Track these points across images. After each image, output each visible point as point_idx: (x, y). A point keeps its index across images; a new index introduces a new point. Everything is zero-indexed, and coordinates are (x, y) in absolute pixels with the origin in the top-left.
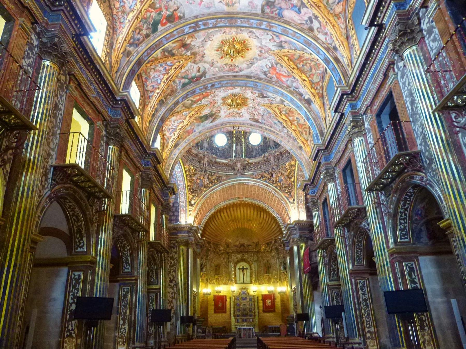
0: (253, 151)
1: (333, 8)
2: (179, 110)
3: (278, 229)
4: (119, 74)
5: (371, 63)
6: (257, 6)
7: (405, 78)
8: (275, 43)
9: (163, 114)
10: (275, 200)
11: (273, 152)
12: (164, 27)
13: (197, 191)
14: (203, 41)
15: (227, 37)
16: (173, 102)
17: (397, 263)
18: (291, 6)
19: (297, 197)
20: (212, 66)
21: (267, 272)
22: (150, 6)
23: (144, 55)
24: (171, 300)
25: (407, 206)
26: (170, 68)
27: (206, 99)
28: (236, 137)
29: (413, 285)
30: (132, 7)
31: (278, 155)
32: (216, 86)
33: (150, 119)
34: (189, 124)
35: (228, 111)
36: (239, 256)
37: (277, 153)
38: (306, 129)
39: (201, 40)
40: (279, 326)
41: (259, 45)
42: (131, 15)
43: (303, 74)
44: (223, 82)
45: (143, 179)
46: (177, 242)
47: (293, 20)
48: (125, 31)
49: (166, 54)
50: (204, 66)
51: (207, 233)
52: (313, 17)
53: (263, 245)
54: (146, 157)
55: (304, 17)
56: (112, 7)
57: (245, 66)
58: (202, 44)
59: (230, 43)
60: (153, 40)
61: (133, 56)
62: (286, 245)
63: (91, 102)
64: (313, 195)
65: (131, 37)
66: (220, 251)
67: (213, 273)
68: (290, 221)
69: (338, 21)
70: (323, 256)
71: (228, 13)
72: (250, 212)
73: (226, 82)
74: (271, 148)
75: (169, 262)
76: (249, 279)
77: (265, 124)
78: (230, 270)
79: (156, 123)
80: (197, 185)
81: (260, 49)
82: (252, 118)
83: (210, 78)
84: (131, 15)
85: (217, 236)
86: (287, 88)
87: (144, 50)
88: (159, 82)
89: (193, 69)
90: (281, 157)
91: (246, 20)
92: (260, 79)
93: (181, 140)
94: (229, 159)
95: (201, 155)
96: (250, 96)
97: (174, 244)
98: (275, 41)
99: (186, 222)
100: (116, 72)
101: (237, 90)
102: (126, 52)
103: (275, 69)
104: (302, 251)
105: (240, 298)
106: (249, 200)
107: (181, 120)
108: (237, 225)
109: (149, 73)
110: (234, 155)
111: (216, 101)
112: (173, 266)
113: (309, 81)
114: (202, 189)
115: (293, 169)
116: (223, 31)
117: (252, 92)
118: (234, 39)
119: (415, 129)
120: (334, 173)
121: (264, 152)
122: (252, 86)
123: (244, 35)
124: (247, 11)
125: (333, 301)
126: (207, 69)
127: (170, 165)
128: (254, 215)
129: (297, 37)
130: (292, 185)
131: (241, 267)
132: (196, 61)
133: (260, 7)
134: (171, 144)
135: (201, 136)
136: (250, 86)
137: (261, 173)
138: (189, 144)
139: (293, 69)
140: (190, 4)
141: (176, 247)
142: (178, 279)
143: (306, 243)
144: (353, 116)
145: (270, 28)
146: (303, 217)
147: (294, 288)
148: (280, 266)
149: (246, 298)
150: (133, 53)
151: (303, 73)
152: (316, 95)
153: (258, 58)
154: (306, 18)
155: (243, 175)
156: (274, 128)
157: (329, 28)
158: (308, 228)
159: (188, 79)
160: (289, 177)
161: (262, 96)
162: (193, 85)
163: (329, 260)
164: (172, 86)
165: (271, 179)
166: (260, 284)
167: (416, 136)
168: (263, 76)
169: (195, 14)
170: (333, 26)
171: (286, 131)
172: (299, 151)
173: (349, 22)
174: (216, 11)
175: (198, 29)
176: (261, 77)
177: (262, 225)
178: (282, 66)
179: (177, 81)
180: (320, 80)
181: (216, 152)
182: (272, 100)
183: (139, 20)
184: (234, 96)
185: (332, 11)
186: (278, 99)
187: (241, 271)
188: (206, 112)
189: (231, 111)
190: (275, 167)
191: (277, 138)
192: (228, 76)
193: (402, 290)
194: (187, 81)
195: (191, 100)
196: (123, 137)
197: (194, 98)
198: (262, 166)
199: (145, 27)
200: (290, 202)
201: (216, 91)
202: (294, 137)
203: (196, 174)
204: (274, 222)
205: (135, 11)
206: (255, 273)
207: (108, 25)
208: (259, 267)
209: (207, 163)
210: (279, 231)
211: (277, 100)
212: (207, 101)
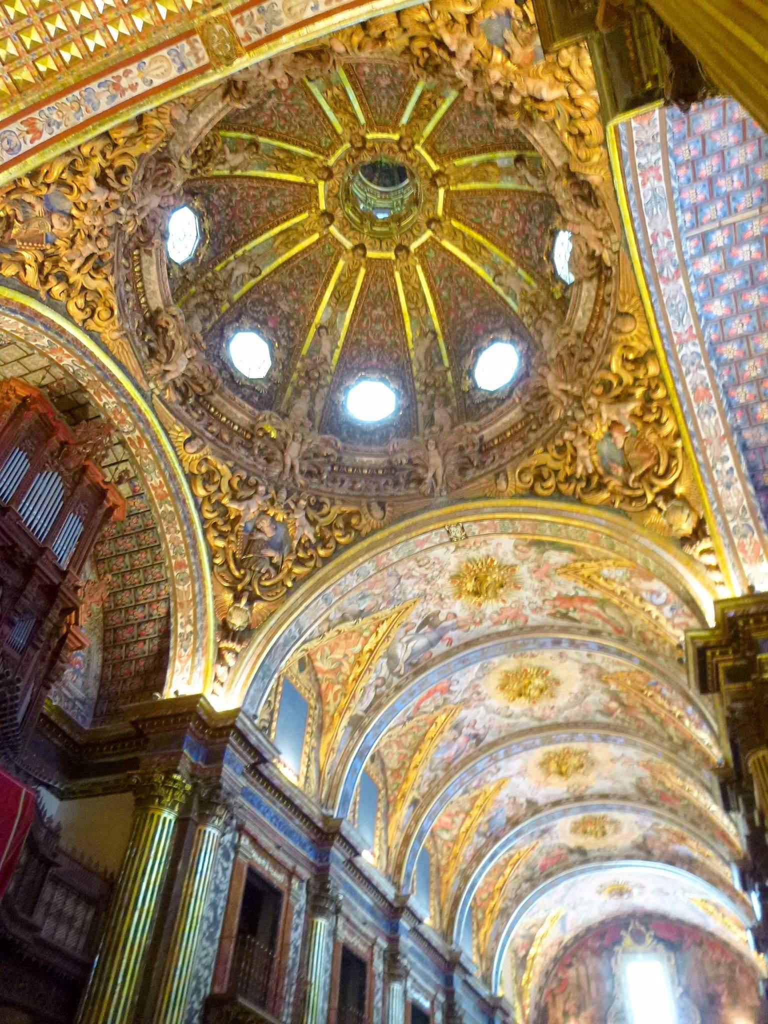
8: (466, 723)
41: (487, 702)
96: (453, 604)
103: (442, 693)
111: (534, 576)
117: (455, 616)
153: (477, 682)
161: (429, 621)
201: (540, 603)
212: (559, 584)
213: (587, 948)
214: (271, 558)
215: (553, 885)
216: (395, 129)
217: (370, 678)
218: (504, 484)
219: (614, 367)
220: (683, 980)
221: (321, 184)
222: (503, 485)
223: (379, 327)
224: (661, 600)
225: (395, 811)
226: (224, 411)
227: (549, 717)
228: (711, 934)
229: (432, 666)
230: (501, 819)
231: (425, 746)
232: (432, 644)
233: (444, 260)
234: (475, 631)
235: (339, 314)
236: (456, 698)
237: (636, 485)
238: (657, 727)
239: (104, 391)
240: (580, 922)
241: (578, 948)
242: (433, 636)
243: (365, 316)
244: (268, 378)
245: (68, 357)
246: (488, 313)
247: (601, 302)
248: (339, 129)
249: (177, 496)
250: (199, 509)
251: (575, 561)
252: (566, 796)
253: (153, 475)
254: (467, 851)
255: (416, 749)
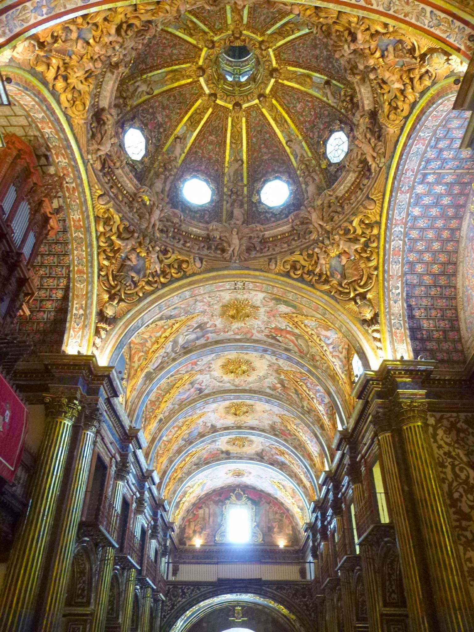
41: (212, 373)
117: (215, 326)
161: (201, 327)
201: (263, 329)
211: (182, 336)
212: (279, 322)
213: (212, 500)
214: (133, 277)
215: (209, 468)
216: (263, 34)
217: (162, 352)
218: (274, 266)
219: (354, 224)
220: (257, 520)
221: (205, 49)
222: (273, 266)
223: (210, 147)
224: (329, 342)
225: (149, 424)
226: (121, 180)
227: (242, 386)
228: (276, 499)
229: (195, 350)
230: (196, 433)
231: (172, 391)
232: (197, 339)
233: (260, 120)
234: (223, 336)
235: (190, 132)
236: (197, 368)
237: (346, 286)
238: (297, 400)
239: (63, 155)
240: (211, 487)
241: (207, 500)
242: (200, 334)
243: (204, 138)
244: (142, 162)
245: (50, 128)
246: (277, 161)
247: (357, 186)
248: (229, 21)
249: (88, 230)
250: (98, 239)
251: (294, 313)
252: (233, 425)
253: (76, 213)
254: (175, 447)
255: (168, 392)
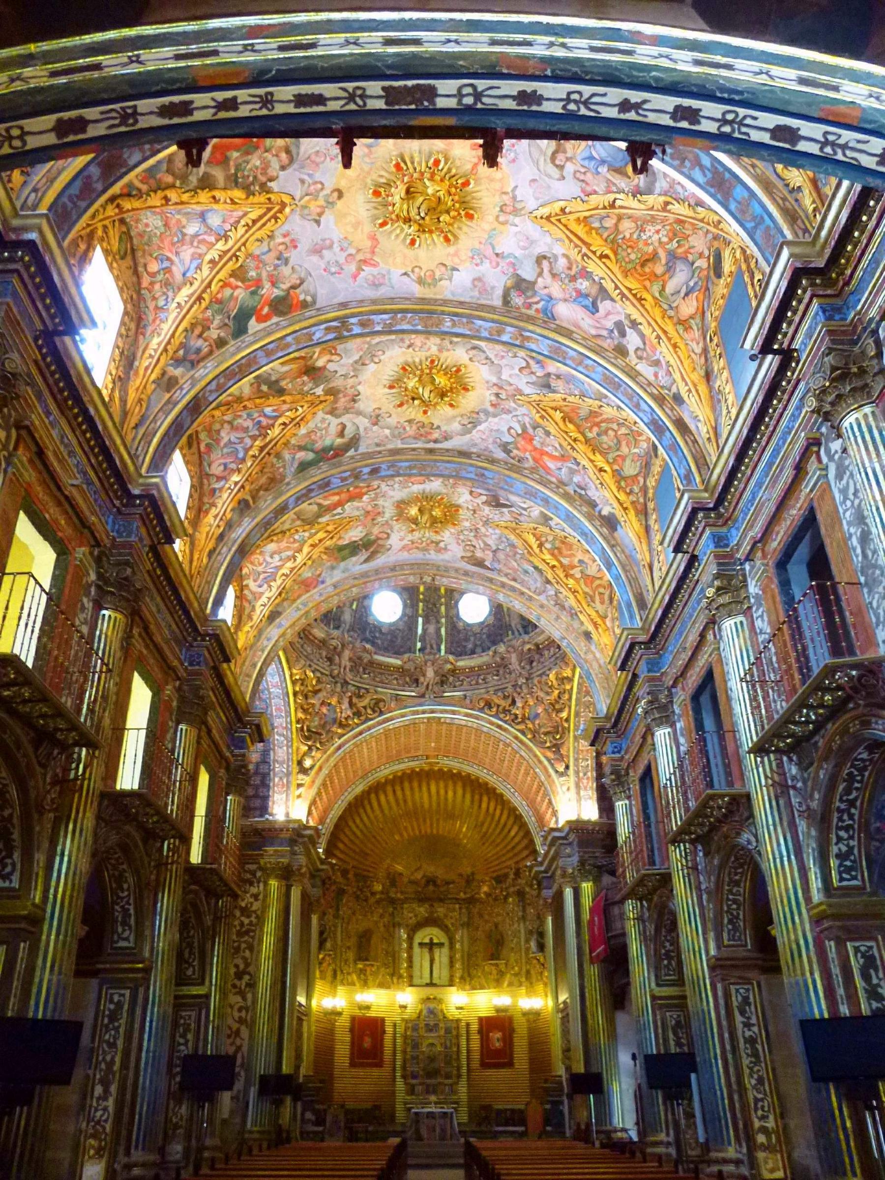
0: (467, 639)
1: (674, 305)
2: (287, 526)
3: (526, 842)
4: (141, 431)
5: (765, 439)
6: (493, 288)
7: (846, 478)
9: (244, 535)
10: (519, 765)
11: (517, 643)
12: (263, 325)
13: (320, 734)
14: (356, 362)
15: (418, 356)
16: (274, 506)
17: (832, 943)
18: (574, 294)
19: (576, 760)
20: (375, 424)
21: (494, 956)
22: (233, 274)
23: (209, 388)
24: (235, 1026)
25: (854, 794)
26: (271, 422)
27: (356, 504)
28: (424, 601)
29: (875, 1005)
30: (188, 275)
31: (529, 650)
32: (383, 473)
33: (211, 546)
34: (310, 562)
35: (410, 537)
36: (422, 909)
37: (527, 647)
38: (602, 590)
39: (351, 361)
40: (522, 1107)
41: (494, 380)
42: (186, 291)
43: (597, 454)
44: (400, 464)
45: (182, 700)
46: (261, 868)
47: (579, 328)
48: (166, 328)
49: (264, 388)
50: (355, 423)
51: (341, 846)
52: (626, 322)
53: (483, 882)
54: (195, 644)
55: (604, 322)
56: (141, 269)
57: (456, 426)
58: (355, 370)
59: (422, 370)
60: (234, 354)
61: (181, 389)
62: (545, 884)
63: (67, 498)
64: (618, 755)
65: (181, 343)
66: (373, 894)
67: (351, 955)
68: (557, 822)
69: (686, 336)
70: (640, 919)
71: (423, 301)
72: (455, 793)
73: (407, 464)
74: (513, 633)
75: (236, 923)
76: (445, 973)
77: (500, 571)
78: (397, 949)
79: (226, 556)
80: (321, 719)
81: (495, 390)
82: (469, 554)
83: (368, 453)
84: (186, 291)
85: (367, 854)
86: (558, 487)
87: (211, 376)
88: (241, 455)
89: (326, 429)
90: (537, 657)
91: (465, 320)
92: (493, 461)
93: (285, 603)
94: (406, 656)
95: (334, 643)
97: (253, 874)
98: (532, 373)
99: (287, 815)
100: (136, 427)
101: (435, 485)
102: (166, 377)
103: (531, 440)
104: (587, 902)
105: (422, 1025)
106: (455, 765)
107: (290, 553)
108: (419, 826)
109: (218, 432)
110: (419, 645)
111: (381, 510)
112: (247, 933)
113: (613, 471)
114: (334, 729)
115: (568, 687)
116: (407, 343)
117: (471, 493)
118: (432, 362)
119: (871, 603)
120: (672, 702)
121: (494, 643)
122: (472, 476)
123: (459, 354)
124: (468, 300)
125: (666, 1040)
126: (361, 430)
127: (255, 665)
128: (463, 801)
129: (586, 367)
130: (564, 728)
131: (427, 940)
132: (336, 409)
133: (499, 292)
134: (260, 611)
135: (337, 594)
136: (469, 476)
137: (485, 696)
138: (307, 612)
139: (575, 440)
140: (332, 274)
141: (259, 882)
142: (258, 968)
143: (597, 880)
144: (719, 564)
145: (522, 341)
146: (590, 812)
147: (565, 1002)
148: (527, 941)
149: (436, 1025)
150: (181, 382)
151: (601, 453)
152: (630, 507)
153: (491, 409)
154: (610, 324)
155: (439, 698)
156: (522, 583)
157: (665, 350)
158: (603, 840)
159: (312, 451)
160: (557, 707)
161: (496, 503)
162: (324, 466)
163: (657, 930)
164: (273, 465)
165: (509, 711)
166: (474, 988)
167: (874, 620)
168: (500, 455)
169: (341, 299)
170: (675, 346)
171: (553, 593)
172: (582, 644)
173: (711, 340)
174: (393, 296)
175: (346, 334)
176: (495, 456)
177: (484, 830)
178: (548, 433)
179: (287, 456)
180: (640, 472)
181: (375, 637)
182: (521, 514)
183: (204, 305)
184: (427, 500)
185: (671, 313)
186: (536, 511)
187: (426, 951)
188: (355, 534)
189: (417, 535)
190: (522, 681)
191: (529, 608)
192: (414, 449)
193: (846, 1018)
194: (311, 456)
195: (319, 505)
196: (140, 590)
197: (325, 498)
198: (489, 677)
199: (216, 323)
200: (557, 772)
202: (571, 608)
203: (320, 690)
204: (515, 822)
205: (196, 284)
206: (462, 956)
207: (126, 313)
208: (473, 940)
209: (348, 664)
210: (526, 847)
212: (358, 508)
